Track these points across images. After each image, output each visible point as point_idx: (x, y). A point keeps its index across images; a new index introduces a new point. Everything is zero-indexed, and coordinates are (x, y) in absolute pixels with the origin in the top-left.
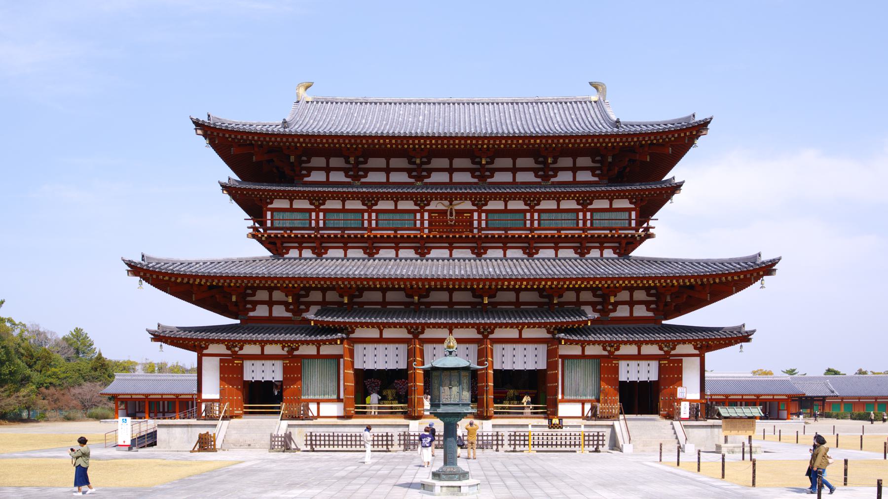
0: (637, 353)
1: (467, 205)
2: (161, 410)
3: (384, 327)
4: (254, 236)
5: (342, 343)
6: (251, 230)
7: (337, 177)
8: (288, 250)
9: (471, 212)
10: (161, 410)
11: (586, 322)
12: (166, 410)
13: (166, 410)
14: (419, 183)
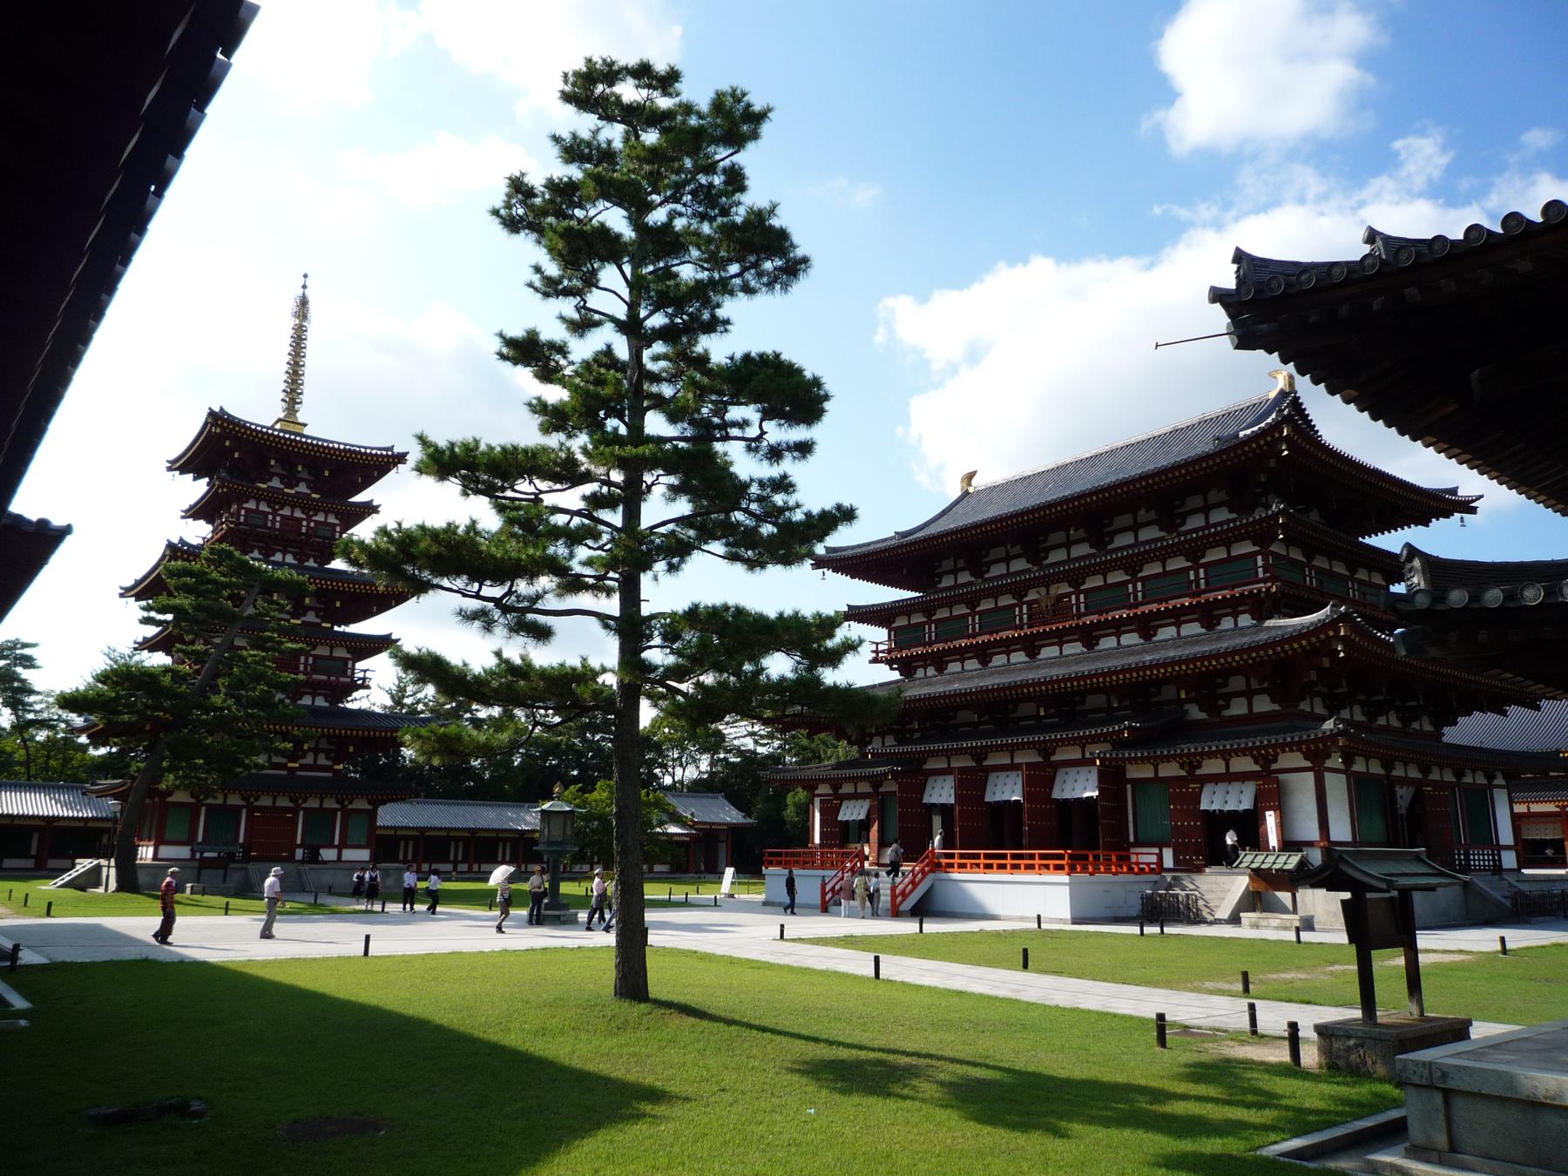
0: (1224, 771)
1: (1064, 588)
2: (452, 858)
3: (952, 754)
4: (875, 661)
5: (894, 778)
6: (874, 655)
7: (1019, 565)
8: (915, 669)
9: (1068, 595)
10: (452, 858)
11: (1121, 732)
12: (460, 858)
13: (460, 858)
14: (1035, 568)
